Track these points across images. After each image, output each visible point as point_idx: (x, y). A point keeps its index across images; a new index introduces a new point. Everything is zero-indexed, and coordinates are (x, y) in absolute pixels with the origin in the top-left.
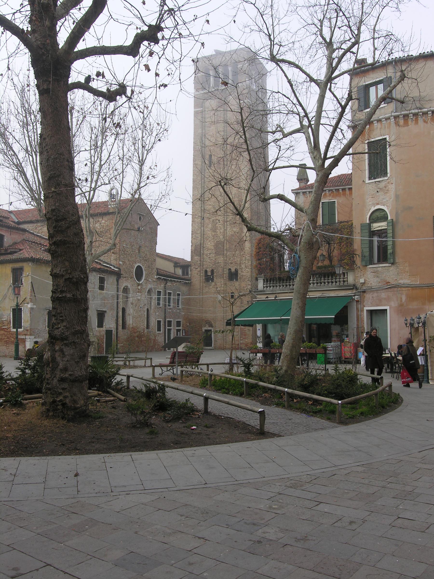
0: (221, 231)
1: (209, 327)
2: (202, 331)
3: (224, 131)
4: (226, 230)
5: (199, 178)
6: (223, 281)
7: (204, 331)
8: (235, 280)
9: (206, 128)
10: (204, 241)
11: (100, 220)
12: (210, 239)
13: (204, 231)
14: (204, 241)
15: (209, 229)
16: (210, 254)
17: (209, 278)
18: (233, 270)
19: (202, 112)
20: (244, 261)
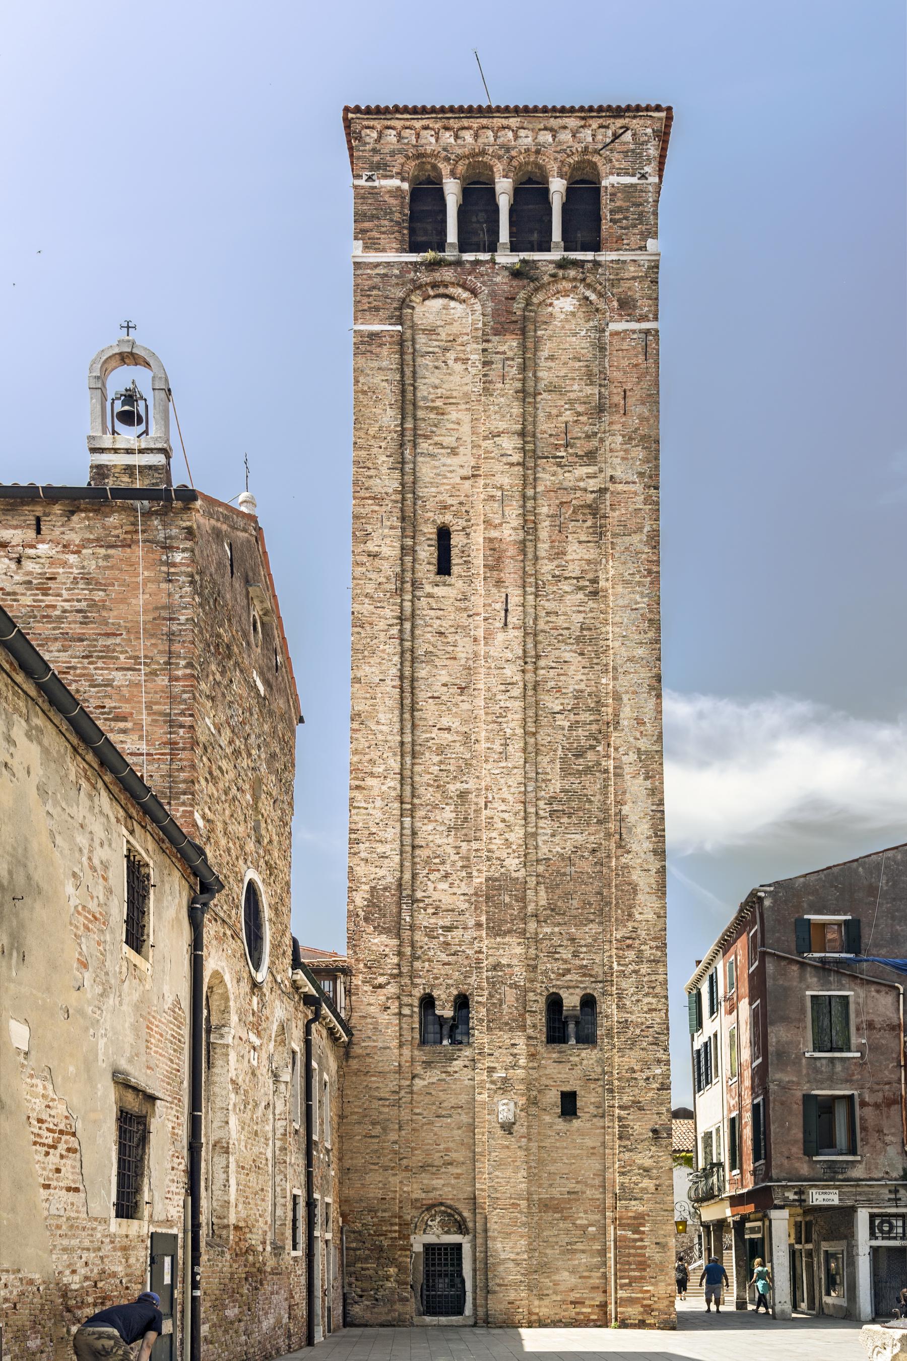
0: (512, 837)
2: (408, 1247)
3: (522, 434)
4: (535, 835)
5: (389, 613)
6: (521, 1042)
7: (418, 1248)
9: (420, 414)
10: (414, 876)
12: (448, 867)
13: (414, 833)
14: (414, 876)
16: (448, 929)
17: (444, 1025)
18: (571, 1000)
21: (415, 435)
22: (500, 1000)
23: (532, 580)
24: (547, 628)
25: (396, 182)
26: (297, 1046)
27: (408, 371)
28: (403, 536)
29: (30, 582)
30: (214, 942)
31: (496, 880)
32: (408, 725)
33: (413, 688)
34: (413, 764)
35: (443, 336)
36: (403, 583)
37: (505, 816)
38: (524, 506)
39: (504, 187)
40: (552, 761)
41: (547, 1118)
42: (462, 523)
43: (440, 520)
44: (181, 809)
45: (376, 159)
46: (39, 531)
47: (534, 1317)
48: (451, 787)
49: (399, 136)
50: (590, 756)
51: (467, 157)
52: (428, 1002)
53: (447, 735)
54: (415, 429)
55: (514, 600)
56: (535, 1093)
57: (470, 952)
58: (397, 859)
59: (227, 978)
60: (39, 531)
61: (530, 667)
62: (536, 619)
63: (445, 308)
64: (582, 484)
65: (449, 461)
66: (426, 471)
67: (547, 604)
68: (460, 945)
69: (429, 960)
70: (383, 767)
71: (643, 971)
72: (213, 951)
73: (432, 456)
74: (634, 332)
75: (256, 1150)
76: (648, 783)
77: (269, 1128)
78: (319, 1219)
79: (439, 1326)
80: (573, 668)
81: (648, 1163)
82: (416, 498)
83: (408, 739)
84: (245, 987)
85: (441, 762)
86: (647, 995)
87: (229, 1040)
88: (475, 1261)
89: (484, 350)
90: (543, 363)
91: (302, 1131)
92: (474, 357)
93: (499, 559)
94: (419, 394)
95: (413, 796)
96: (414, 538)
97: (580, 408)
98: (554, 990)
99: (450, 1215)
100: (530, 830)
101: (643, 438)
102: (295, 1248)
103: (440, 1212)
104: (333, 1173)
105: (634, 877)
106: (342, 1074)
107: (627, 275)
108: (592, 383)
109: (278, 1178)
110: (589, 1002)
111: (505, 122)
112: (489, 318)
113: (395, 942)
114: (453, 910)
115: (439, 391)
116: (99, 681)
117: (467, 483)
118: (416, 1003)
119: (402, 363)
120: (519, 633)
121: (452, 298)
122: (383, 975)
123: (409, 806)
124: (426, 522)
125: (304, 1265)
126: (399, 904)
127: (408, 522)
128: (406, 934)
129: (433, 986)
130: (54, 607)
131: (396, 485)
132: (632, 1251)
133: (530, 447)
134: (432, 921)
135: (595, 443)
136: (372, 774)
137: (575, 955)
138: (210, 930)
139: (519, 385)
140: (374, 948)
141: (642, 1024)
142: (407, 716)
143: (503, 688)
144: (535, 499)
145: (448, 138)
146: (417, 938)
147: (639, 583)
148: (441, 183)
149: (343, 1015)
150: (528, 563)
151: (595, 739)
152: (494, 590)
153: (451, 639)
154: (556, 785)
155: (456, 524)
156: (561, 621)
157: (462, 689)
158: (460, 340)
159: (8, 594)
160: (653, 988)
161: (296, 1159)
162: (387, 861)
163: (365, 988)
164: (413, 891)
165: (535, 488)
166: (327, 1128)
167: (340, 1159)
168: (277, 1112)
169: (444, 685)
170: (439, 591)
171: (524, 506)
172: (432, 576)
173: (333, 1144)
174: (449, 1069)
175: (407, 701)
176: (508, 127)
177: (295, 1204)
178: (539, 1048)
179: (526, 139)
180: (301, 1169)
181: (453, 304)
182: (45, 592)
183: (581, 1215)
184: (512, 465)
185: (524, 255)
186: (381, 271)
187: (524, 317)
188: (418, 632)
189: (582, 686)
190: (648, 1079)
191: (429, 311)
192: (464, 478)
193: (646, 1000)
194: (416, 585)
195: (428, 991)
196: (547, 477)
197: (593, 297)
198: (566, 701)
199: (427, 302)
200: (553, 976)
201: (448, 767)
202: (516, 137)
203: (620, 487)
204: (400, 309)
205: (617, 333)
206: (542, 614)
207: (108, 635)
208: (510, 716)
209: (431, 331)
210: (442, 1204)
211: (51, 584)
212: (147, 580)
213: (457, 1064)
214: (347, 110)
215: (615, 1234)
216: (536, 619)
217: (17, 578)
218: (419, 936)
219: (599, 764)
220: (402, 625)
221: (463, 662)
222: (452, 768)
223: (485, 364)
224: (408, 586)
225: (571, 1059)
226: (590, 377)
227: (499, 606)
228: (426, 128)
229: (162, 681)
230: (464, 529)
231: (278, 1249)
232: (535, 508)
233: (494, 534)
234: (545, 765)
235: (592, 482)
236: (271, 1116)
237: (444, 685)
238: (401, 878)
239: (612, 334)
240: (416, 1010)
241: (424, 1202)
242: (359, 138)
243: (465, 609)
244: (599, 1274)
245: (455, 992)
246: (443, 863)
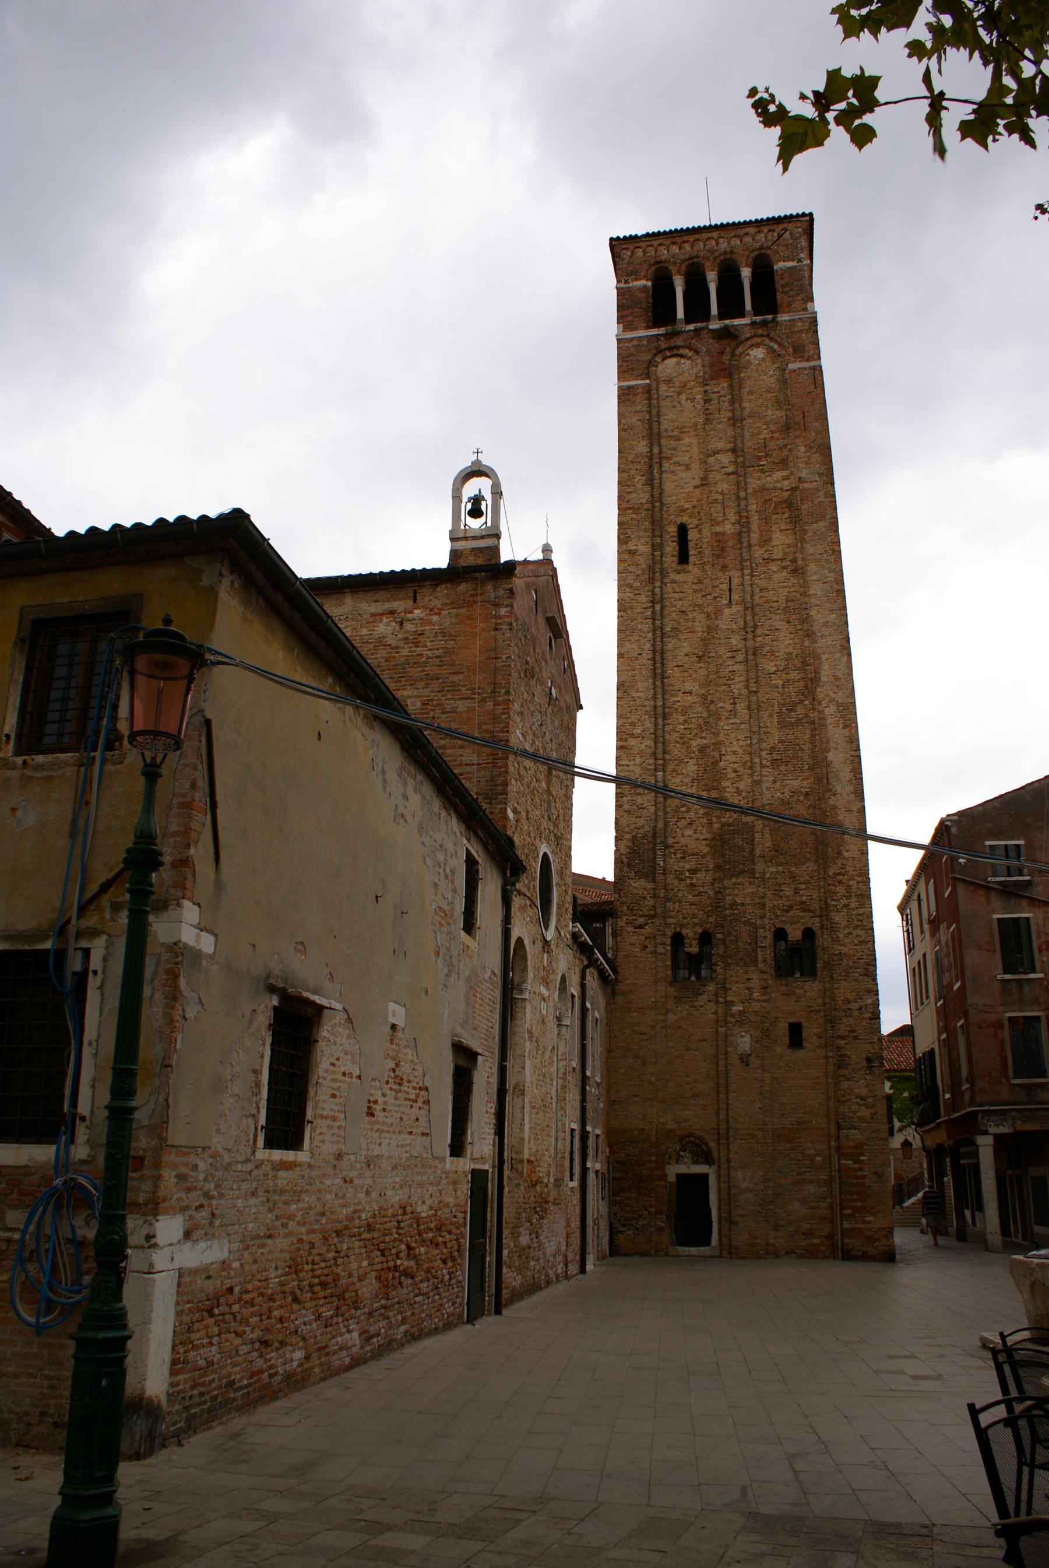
0: (742, 786)
1: (697, 1162)
2: (664, 1177)
3: (734, 450)
4: (759, 783)
5: (643, 598)
6: (755, 977)
7: (672, 1178)
8: (798, 975)
9: (663, 442)
10: (666, 824)
11: (398, 605)
12: (692, 815)
14: (666, 824)
15: (686, 780)
16: (693, 871)
18: (795, 934)
19: (648, 390)
20: (844, 901)
21: (660, 458)
22: (736, 936)
23: (748, 563)
24: (761, 602)
25: (643, 282)
26: (575, 991)
27: (654, 412)
28: (654, 536)
29: (407, 638)
30: (518, 913)
31: (730, 825)
32: (660, 690)
33: (662, 659)
34: (664, 725)
35: (677, 384)
36: (654, 573)
37: (736, 766)
38: (739, 506)
39: (712, 279)
40: (771, 716)
41: (778, 1050)
42: (695, 521)
43: (679, 521)
44: (499, 806)
45: (631, 268)
46: (415, 601)
47: (771, 1248)
48: (694, 743)
49: (645, 252)
50: (800, 709)
51: (687, 260)
52: (678, 940)
53: (689, 698)
54: (660, 453)
55: (736, 581)
56: (767, 1025)
57: (710, 892)
58: (652, 809)
59: (526, 942)
60: (415, 601)
61: (750, 636)
62: (752, 596)
63: (678, 364)
64: (779, 485)
65: (684, 475)
66: (668, 487)
67: (760, 582)
68: (703, 887)
69: (680, 902)
70: (641, 728)
71: (852, 905)
72: (517, 921)
73: (673, 472)
74: (805, 369)
75: (544, 1090)
76: (846, 732)
77: (554, 1069)
78: (591, 1151)
79: (689, 1256)
80: (782, 634)
81: (863, 1091)
82: (662, 505)
83: (660, 703)
84: (539, 944)
85: (685, 722)
86: (857, 926)
87: (526, 996)
88: (719, 1191)
89: (706, 392)
90: (745, 397)
91: (578, 1069)
92: (699, 397)
93: (723, 549)
94: (662, 428)
95: (664, 753)
96: (661, 536)
97: (773, 427)
98: (781, 926)
99: (699, 1146)
100: (756, 778)
102: (571, 1180)
103: (691, 1141)
104: (602, 1105)
105: (840, 818)
106: (611, 1009)
107: (796, 329)
108: (780, 409)
109: (559, 1114)
110: (808, 934)
111: (710, 235)
112: (707, 369)
113: (650, 885)
114: (697, 854)
115: (676, 424)
116: (448, 709)
117: (698, 491)
118: (669, 941)
119: (650, 406)
120: (740, 608)
121: (681, 356)
122: (641, 916)
123: (661, 762)
124: (670, 523)
125: (578, 1195)
126: (654, 850)
127: (657, 526)
128: (660, 878)
129: (682, 926)
130: (421, 655)
131: (647, 496)
132: (854, 1181)
133: (740, 460)
134: (681, 864)
135: (785, 453)
136: (633, 736)
137: (796, 892)
138: (517, 902)
139: (730, 414)
140: (635, 891)
141: (854, 955)
142: (658, 683)
143: (730, 654)
144: (746, 499)
145: (675, 249)
146: (669, 881)
147: (826, 561)
148: (671, 278)
149: (610, 955)
150: (744, 550)
151: (803, 694)
152: (720, 574)
153: (690, 616)
154: (775, 736)
155: (691, 522)
156: (770, 595)
157: (700, 657)
158: (689, 386)
159: (394, 648)
160: (861, 921)
161: (573, 1096)
162: (645, 811)
163: (629, 929)
164: (666, 837)
165: (746, 490)
166: (598, 1063)
167: (608, 1092)
168: (560, 1053)
169: (686, 655)
170: (680, 578)
171: (739, 506)
172: (674, 565)
173: (602, 1078)
174: (696, 1004)
175: (659, 671)
176: (712, 238)
177: (572, 1137)
178: (770, 982)
179: (724, 245)
180: (577, 1105)
181: (682, 361)
182: (416, 644)
183: (809, 1145)
184: (729, 474)
185: (727, 322)
186: (635, 343)
187: (731, 365)
188: (666, 612)
189: (790, 649)
190: (860, 1009)
191: (668, 367)
192: (696, 487)
193: (855, 932)
194: (663, 574)
195: (678, 930)
196: (754, 482)
197: (776, 347)
198: (779, 663)
199: (666, 361)
200: (779, 913)
201: (691, 726)
202: (717, 244)
203: (807, 485)
204: (648, 368)
205: (794, 371)
206: (757, 590)
207: (454, 673)
208: (737, 680)
209: (669, 381)
210: (691, 1135)
211: (421, 639)
212: (483, 630)
213: (702, 999)
214: (611, 239)
215: (839, 1163)
216: (752, 596)
217: (400, 636)
218: (671, 879)
219: (806, 716)
220: (653, 607)
221: (700, 635)
222: (693, 726)
223: (706, 401)
224: (658, 575)
225: (797, 991)
226: (778, 404)
227: (725, 587)
228: (661, 245)
229: (489, 705)
230: (697, 526)
231: (558, 1183)
232: (746, 506)
233: (718, 529)
234: (765, 719)
235: (786, 483)
236: (555, 1059)
237: (686, 655)
238: (655, 827)
239: (791, 372)
240: (669, 948)
241: (678, 1133)
242: (619, 257)
243: (701, 591)
244: (826, 1205)
245: (700, 931)
246: (688, 811)
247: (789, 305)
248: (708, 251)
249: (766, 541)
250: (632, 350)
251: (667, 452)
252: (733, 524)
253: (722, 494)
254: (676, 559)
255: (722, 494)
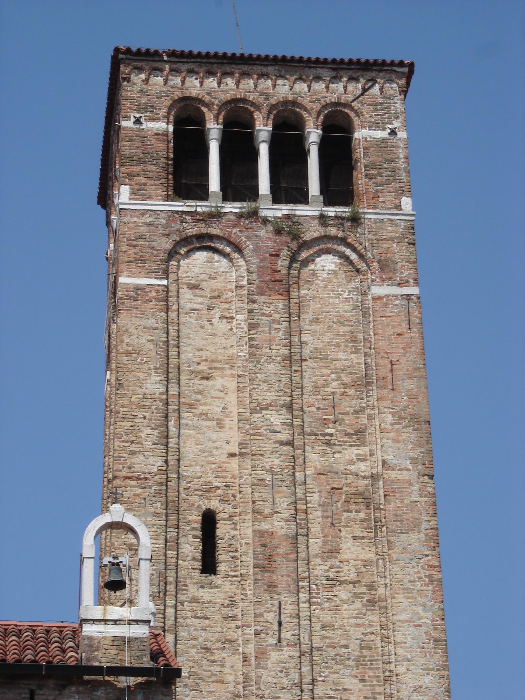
3: (290, 407)
45: (143, 101)
55: (288, 609)
62: (311, 634)
64: (353, 468)
65: (214, 436)
66: (190, 449)
74: (395, 297)
93: (270, 558)
97: (346, 379)
101: (414, 417)
108: (357, 351)
112: (254, 276)
115: (204, 354)
117: (235, 462)
121: (216, 251)
131: (160, 462)
152: (266, 596)
153: (216, 657)
156: (336, 636)
170: (205, 594)
172: (196, 574)
192: (232, 455)
196: (315, 459)
203: (394, 474)
205: (380, 298)
214: (117, 50)
216: (311, 634)
221: (231, 687)
223: (251, 327)
224: (171, 588)
227: (271, 617)
233: (265, 526)
235: (362, 466)
247: (376, 197)
248: (262, 93)
249: (332, 552)
250: (143, 229)
251: (188, 397)
252: (287, 521)
253: (271, 471)
254: (198, 565)
255: (271, 471)
